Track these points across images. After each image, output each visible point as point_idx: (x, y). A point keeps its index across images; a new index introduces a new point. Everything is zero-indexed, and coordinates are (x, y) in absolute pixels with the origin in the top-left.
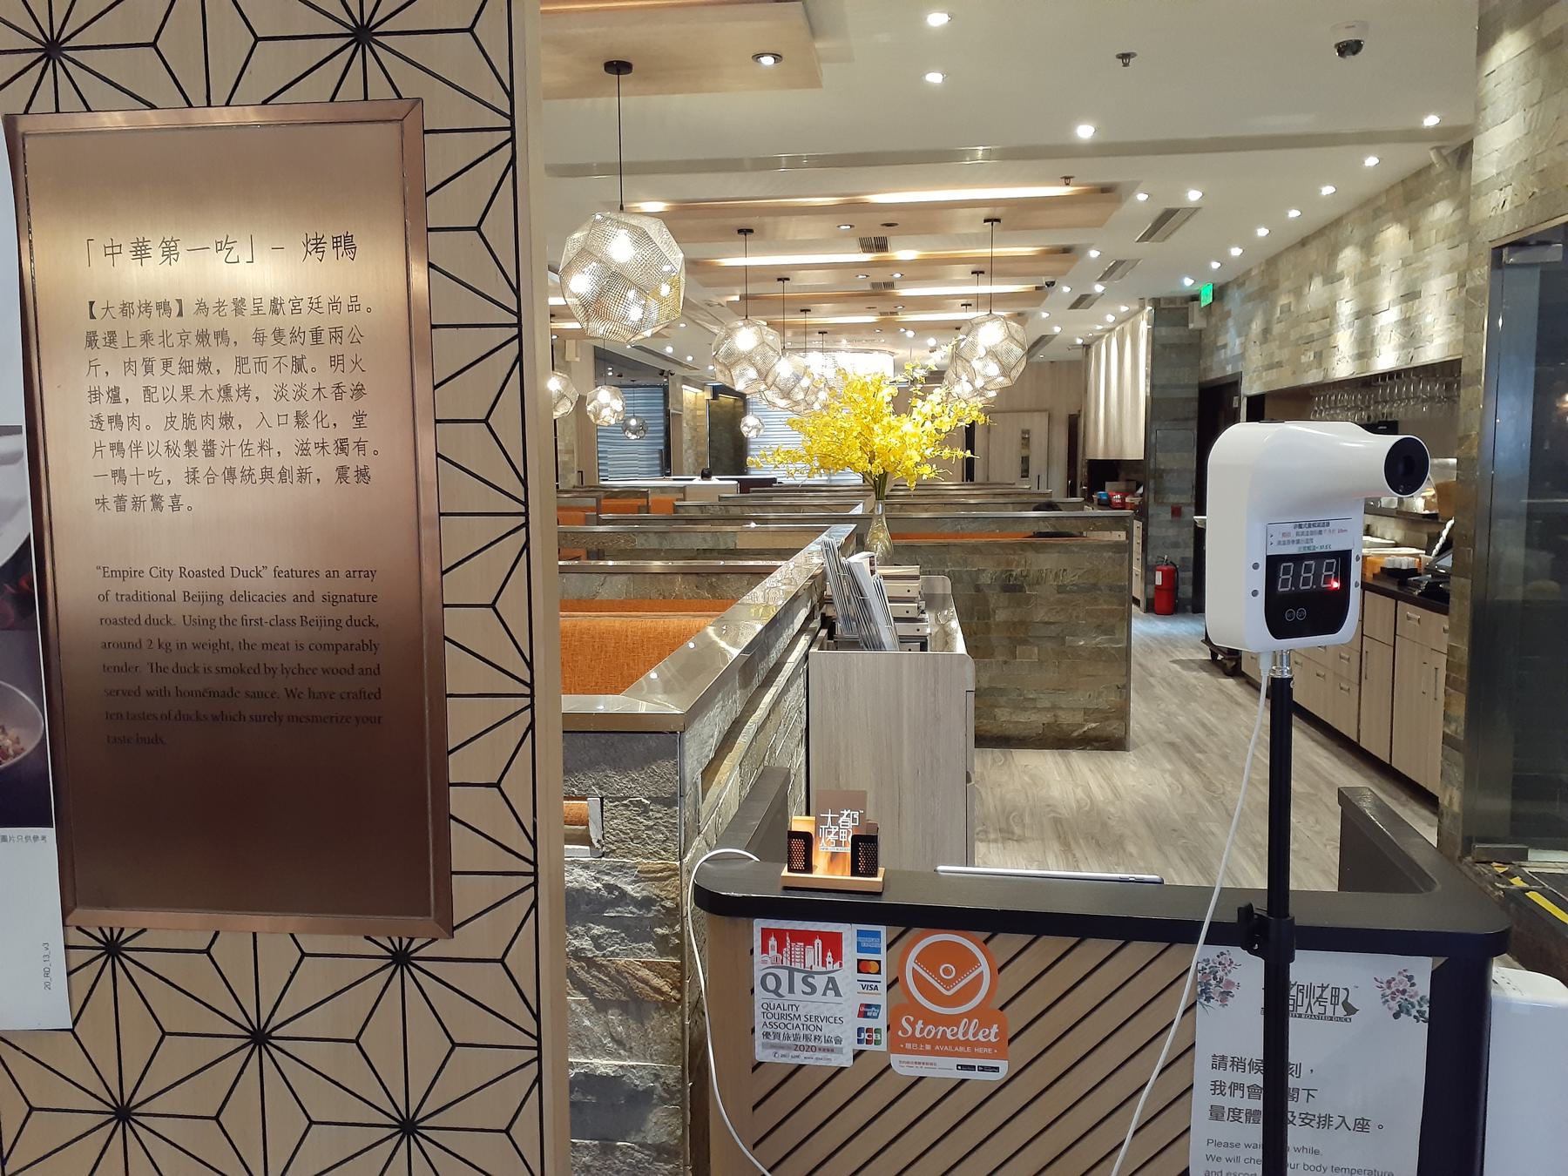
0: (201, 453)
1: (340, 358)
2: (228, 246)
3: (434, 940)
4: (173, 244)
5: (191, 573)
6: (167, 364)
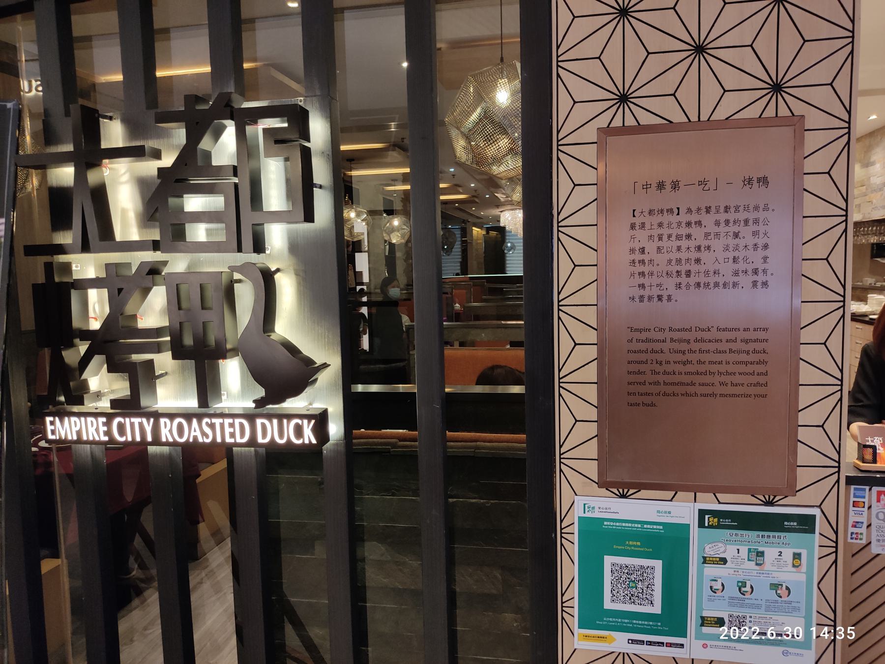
0: (684, 276)
1: (758, 232)
2: (705, 183)
3: (786, 497)
4: (677, 183)
5: (675, 330)
6: (669, 236)
